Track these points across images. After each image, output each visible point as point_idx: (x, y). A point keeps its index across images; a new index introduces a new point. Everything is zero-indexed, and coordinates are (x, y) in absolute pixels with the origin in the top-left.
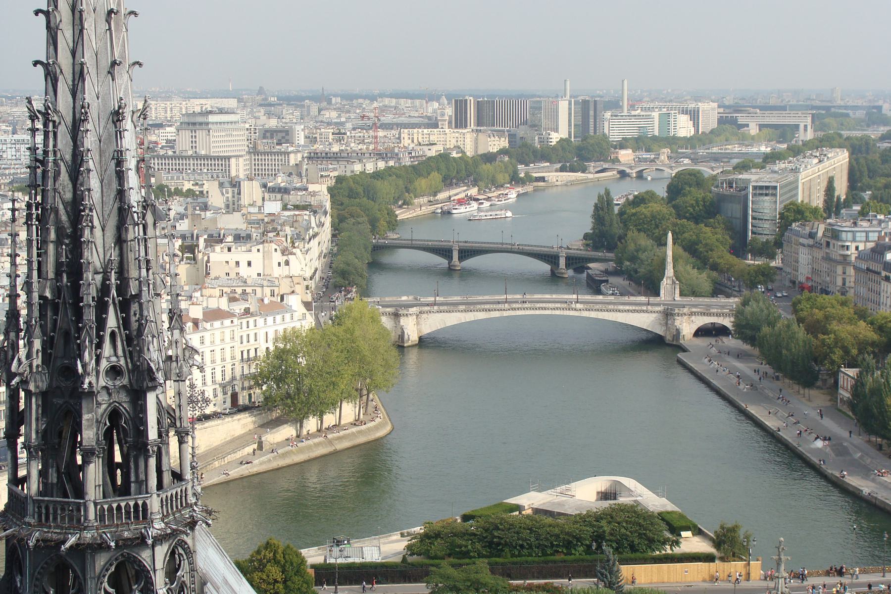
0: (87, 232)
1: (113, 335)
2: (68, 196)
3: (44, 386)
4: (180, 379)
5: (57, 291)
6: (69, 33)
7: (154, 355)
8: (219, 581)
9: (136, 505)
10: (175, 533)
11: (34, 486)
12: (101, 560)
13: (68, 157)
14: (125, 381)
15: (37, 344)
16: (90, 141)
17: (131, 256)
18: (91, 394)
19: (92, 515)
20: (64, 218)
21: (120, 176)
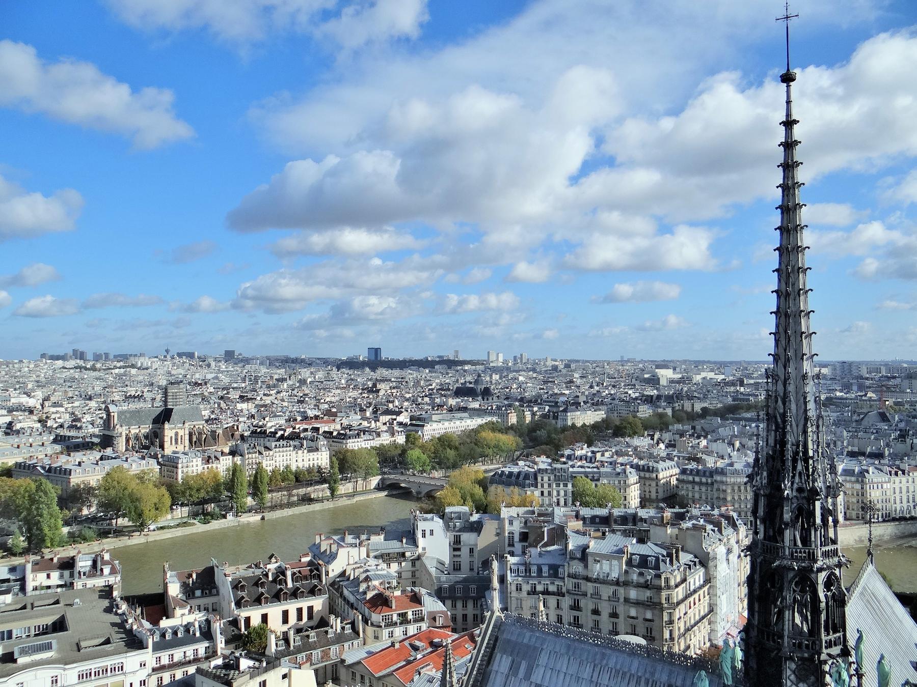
0: (788, 427)
1: (800, 474)
2: (782, 411)
3: (767, 492)
4: (835, 497)
5: (774, 451)
6: (783, 342)
7: (819, 484)
8: (880, 598)
9: (809, 552)
10: (829, 568)
11: (761, 536)
12: (791, 575)
13: (782, 394)
14: (806, 494)
15: (765, 474)
16: (791, 388)
17: (810, 439)
18: (788, 498)
19: (787, 553)
20: (779, 420)
21: (805, 403)
